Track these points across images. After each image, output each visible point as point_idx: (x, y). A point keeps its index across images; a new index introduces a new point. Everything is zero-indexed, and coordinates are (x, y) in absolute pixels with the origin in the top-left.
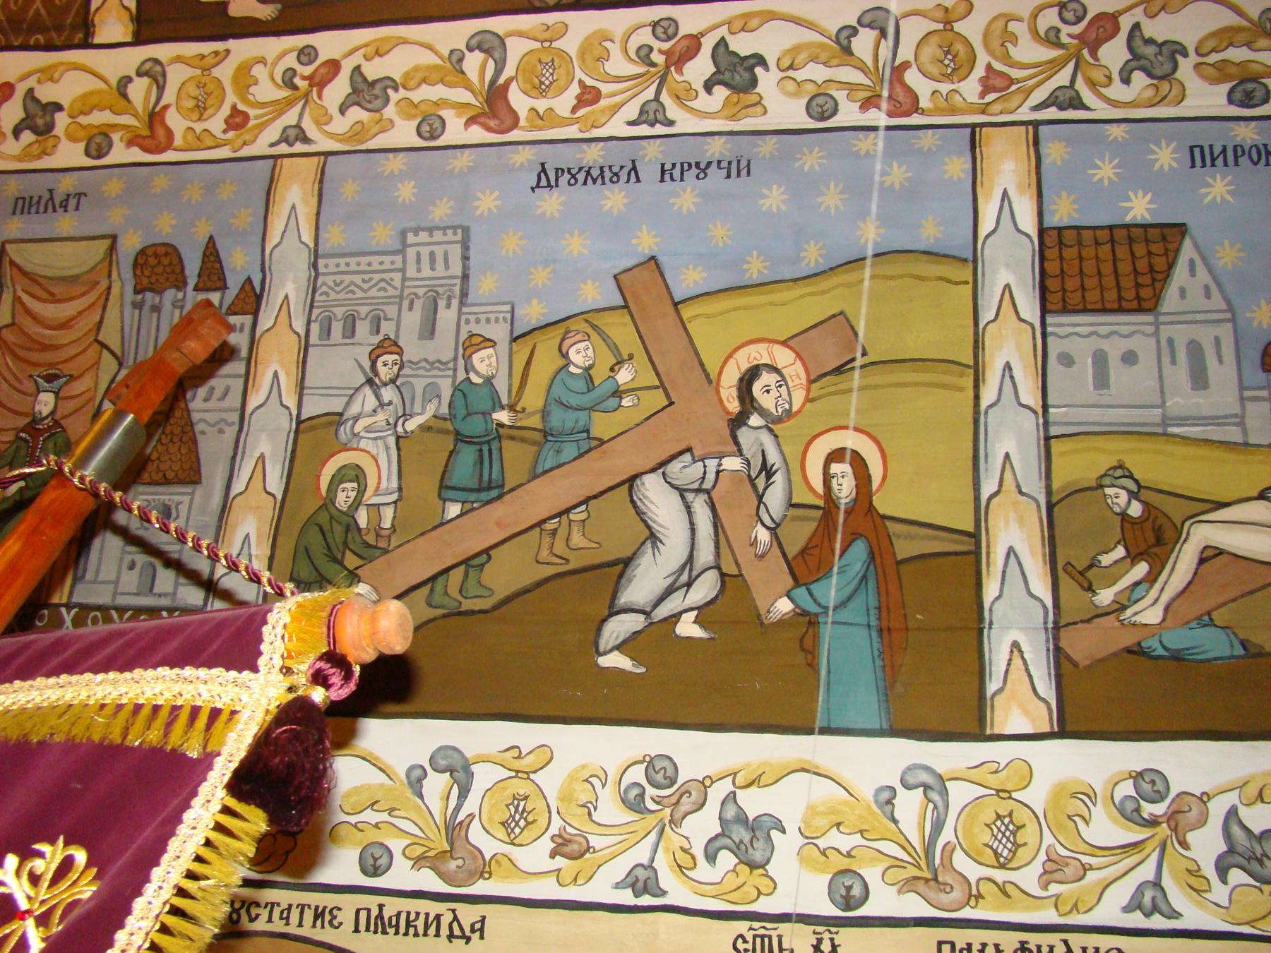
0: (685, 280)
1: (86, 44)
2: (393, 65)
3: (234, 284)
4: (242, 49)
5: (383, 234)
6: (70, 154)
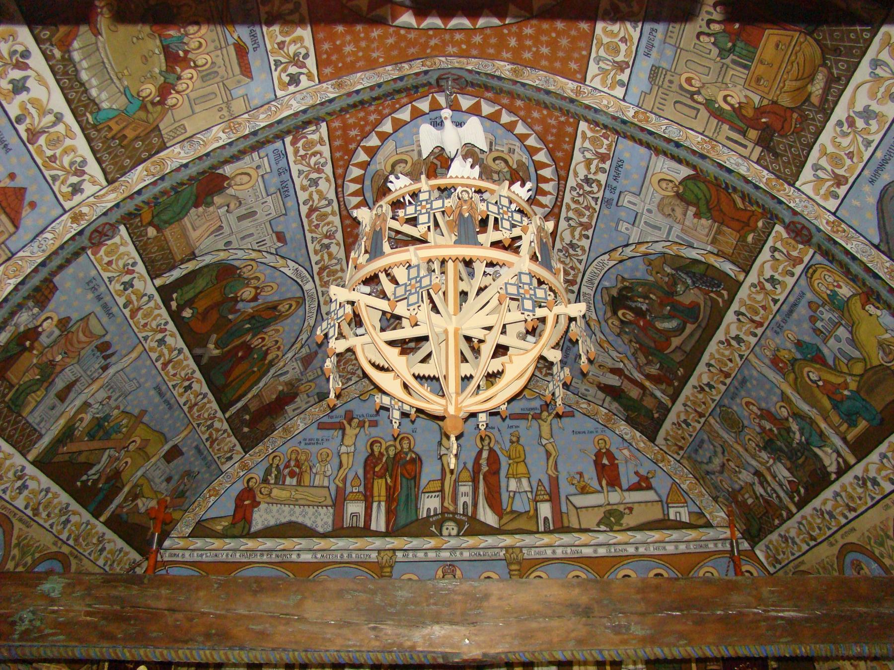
0: (146, 419)
1: (152, 279)
2: (169, 340)
3: (109, 360)
4: (163, 311)
6: (121, 301)
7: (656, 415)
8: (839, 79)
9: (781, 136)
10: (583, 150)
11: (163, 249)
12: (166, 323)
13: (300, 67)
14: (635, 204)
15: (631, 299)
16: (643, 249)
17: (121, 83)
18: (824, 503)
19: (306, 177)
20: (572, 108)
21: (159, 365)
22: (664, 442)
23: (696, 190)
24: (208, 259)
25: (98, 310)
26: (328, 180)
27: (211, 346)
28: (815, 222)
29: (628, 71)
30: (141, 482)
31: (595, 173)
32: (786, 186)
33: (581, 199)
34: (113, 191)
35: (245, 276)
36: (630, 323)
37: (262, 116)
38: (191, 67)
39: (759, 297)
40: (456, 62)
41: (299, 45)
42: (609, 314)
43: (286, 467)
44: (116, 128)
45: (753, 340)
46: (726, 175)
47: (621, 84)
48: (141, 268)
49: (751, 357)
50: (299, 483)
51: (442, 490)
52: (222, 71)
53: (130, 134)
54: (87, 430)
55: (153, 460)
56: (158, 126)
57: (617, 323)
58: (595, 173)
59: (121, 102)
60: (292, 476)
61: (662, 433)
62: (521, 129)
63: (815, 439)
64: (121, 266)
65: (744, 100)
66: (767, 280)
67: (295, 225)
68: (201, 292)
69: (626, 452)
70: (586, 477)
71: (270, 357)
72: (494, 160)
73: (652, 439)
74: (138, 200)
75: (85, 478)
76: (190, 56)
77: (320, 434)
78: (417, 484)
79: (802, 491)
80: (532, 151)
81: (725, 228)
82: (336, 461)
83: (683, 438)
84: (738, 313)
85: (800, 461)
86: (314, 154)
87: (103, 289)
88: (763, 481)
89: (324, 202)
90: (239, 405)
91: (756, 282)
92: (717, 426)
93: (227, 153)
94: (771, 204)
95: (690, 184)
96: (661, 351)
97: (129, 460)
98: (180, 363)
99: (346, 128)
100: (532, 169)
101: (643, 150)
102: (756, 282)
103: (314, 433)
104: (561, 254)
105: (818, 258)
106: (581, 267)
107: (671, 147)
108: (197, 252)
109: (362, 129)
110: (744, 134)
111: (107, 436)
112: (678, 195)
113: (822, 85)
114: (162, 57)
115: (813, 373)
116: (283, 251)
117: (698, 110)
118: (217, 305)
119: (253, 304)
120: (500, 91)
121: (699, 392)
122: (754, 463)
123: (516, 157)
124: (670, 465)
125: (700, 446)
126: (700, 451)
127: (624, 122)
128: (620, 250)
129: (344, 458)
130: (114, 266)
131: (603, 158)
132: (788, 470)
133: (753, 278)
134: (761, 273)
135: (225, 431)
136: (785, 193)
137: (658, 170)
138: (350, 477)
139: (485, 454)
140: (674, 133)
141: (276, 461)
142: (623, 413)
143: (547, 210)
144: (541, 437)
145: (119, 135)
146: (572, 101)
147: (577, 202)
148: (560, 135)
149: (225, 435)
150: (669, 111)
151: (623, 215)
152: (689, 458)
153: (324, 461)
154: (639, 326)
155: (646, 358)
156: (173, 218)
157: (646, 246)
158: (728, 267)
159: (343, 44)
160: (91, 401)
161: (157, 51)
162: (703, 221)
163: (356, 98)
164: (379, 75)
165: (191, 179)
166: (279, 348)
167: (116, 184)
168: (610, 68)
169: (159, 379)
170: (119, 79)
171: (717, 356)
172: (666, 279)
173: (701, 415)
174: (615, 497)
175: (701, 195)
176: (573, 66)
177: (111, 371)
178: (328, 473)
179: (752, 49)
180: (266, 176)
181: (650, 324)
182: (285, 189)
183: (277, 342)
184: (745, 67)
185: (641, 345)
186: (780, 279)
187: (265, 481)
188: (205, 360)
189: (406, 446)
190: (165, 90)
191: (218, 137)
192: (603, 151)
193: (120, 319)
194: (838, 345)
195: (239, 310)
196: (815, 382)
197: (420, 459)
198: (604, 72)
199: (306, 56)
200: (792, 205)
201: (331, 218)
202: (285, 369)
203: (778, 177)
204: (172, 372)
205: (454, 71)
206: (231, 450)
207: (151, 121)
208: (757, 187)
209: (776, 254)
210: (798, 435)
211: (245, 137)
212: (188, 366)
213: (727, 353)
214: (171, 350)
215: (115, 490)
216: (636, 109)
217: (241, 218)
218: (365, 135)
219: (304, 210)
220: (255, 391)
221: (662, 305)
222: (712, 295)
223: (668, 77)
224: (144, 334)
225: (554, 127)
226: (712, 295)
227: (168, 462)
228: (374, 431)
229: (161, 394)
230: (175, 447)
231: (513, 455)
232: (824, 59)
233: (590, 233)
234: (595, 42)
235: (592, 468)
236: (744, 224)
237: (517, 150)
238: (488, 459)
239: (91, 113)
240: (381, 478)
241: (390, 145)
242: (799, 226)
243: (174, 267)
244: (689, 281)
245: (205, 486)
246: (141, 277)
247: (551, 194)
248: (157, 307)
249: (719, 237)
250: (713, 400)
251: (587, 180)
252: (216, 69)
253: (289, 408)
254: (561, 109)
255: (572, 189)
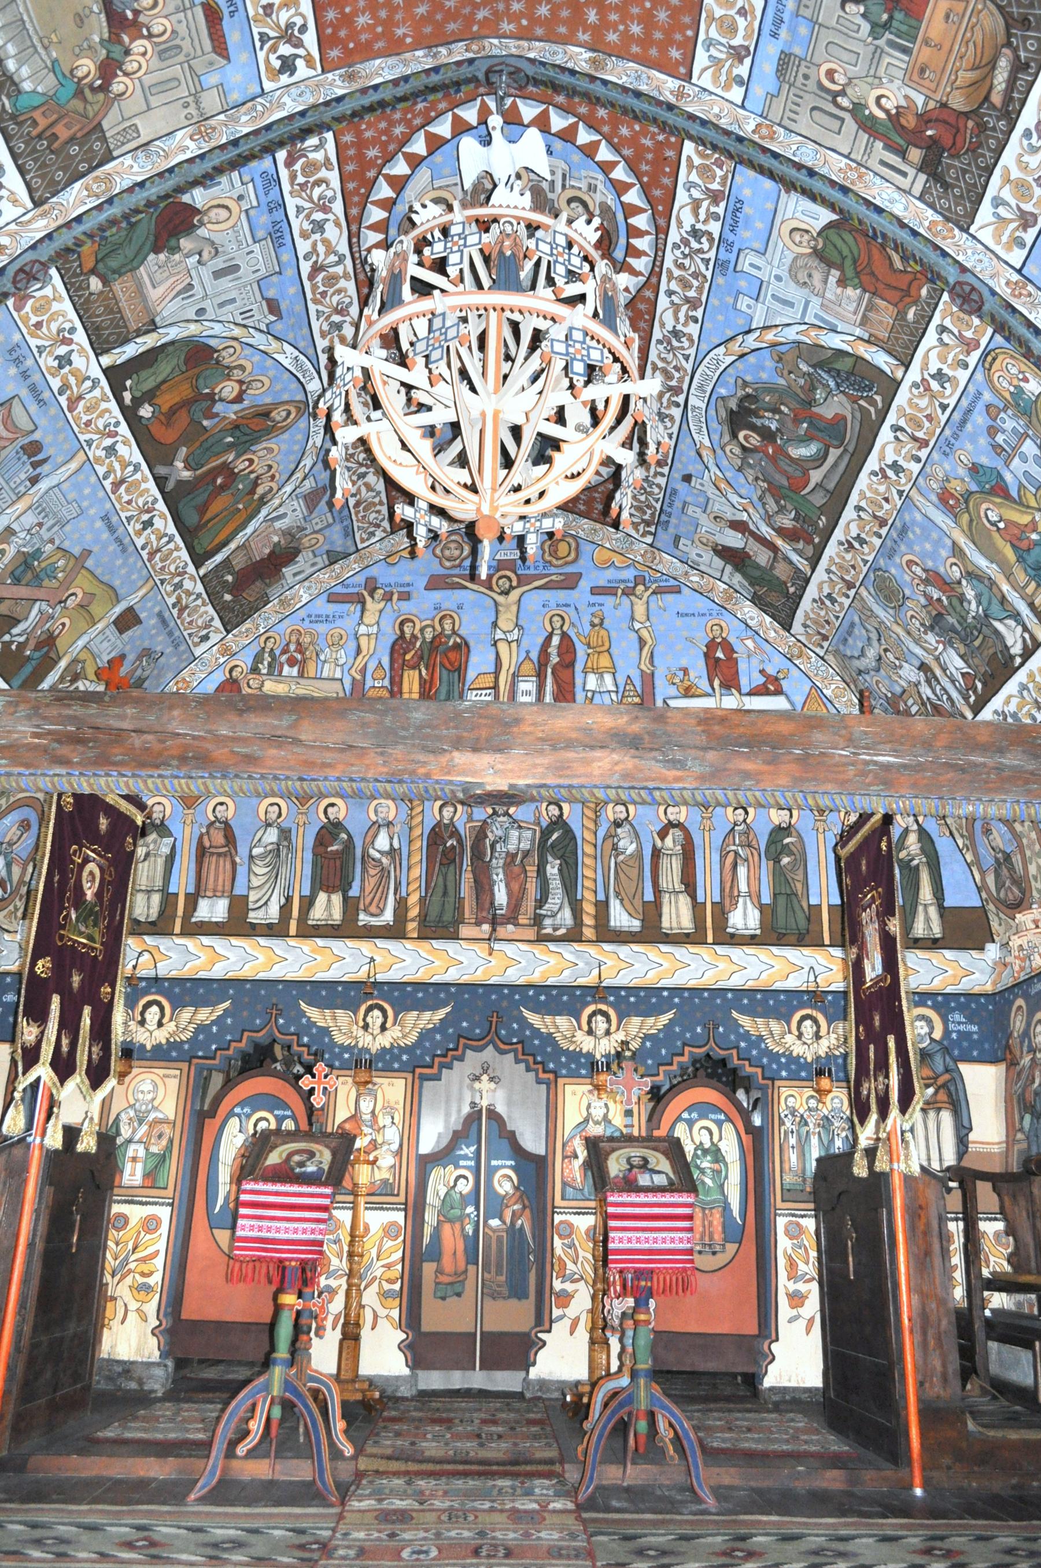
0: (89, 563)
1: (97, 355)
4: (113, 405)
5: (71, 496)
6: (56, 383)
7: (792, 590)
8: (1027, 66)
9: (951, 156)
10: (690, 186)
11: (112, 312)
12: (117, 424)
13: (295, 46)
14: (759, 268)
15: (755, 413)
16: (770, 336)
17: (49, 55)
18: (1007, 702)
19: (308, 217)
20: (671, 118)
21: (107, 484)
22: (802, 630)
23: (839, 243)
24: (173, 333)
25: (24, 393)
26: (337, 224)
27: (179, 464)
28: (991, 283)
29: (748, 61)
30: (82, 657)
31: (705, 222)
32: (956, 231)
33: (687, 262)
34: (44, 215)
35: (226, 362)
36: (754, 450)
37: (244, 119)
38: (143, 37)
39: (923, 403)
40: (512, 46)
41: (292, 11)
42: (727, 438)
43: (284, 652)
44: (43, 123)
45: (915, 468)
46: (875, 216)
47: (740, 81)
48: (81, 337)
49: (914, 493)
50: (301, 675)
51: (495, 687)
52: (186, 45)
53: (63, 133)
54: (10, 569)
55: (100, 626)
56: (100, 124)
57: (737, 451)
58: (705, 222)
59: (47, 84)
60: (291, 665)
61: (800, 615)
62: (605, 154)
63: (995, 608)
64: (54, 331)
65: (903, 103)
66: (933, 377)
67: (293, 290)
68: (164, 382)
69: (749, 643)
70: (692, 674)
71: (260, 490)
72: (569, 201)
73: (787, 626)
74: (78, 230)
75: (7, 638)
76: (142, 19)
77: (332, 608)
78: (462, 679)
79: (979, 685)
80: (620, 188)
81: (878, 301)
82: (352, 645)
83: (828, 622)
84: (896, 428)
85: (977, 643)
86: (318, 183)
87: (29, 362)
88: (931, 679)
89: (333, 258)
90: (219, 558)
91: (918, 380)
92: (871, 601)
93: (198, 170)
94: (933, 257)
95: (832, 234)
96: (797, 491)
97: (67, 621)
98: (137, 484)
99: (361, 144)
100: (620, 217)
101: (768, 184)
102: (918, 380)
103: (322, 607)
104: (661, 347)
105: (999, 339)
106: (688, 367)
107: (802, 177)
108: (157, 319)
109: (384, 146)
110: (903, 154)
111: (37, 580)
112: (816, 253)
113: (1006, 75)
114: (103, 16)
115: (992, 512)
116: (278, 328)
117: (843, 120)
118: (186, 404)
119: (236, 407)
120: (572, 92)
121: (847, 551)
122: (918, 651)
123: (598, 197)
124: (811, 663)
125: (850, 633)
126: (850, 641)
127: (740, 139)
128: (740, 338)
129: (363, 641)
130: (44, 329)
131: (715, 197)
132: (961, 657)
133: (914, 374)
134: (925, 366)
135: (199, 596)
136: (958, 245)
137: (789, 214)
138: (372, 666)
139: (556, 640)
140: (807, 155)
141: (270, 645)
142: (748, 590)
143: (642, 279)
144: (633, 619)
145: (48, 133)
146: (670, 107)
147: (681, 267)
148: (660, 161)
149: (199, 602)
150: (804, 123)
151: (743, 284)
152: (837, 653)
153: (336, 644)
154: (767, 454)
155: (777, 502)
156: (123, 266)
157: (774, 331)
158: (881, 360)
159: (355, 13)
160: (15, 526)
161: (95, 9)
162: (849, 291)
163: (373, 97)
164: (406, 64)
165: (149, 204)
166: (273, 477)
167: (46, 207)
168: (723, 56)
169: (108, 505)
170: (46, 48)
171: (868, 494)
172: (802, 382)
173: (850, 585)
174: (730, 702)
175: (846, 252)
176: (675, 54)
177: (43, 485)
178: (342, 661)
179: (914, 23)
180: (252, 212)
181: (781, 451)
182: (278, 235)
183: (270, 467)
184: (905, 51)
185: (769, 483)
186: (950, 373)
187: (255, 670)
188: (170, 486)
189: (448, 627)
190: (109, 69)
191: (185, 146)
192: (715, 186)
193: (53, 410)
194: (1025, 467)
195: (217, 415)
196: (994, 524)
197: (467, 644)
198: (717, 63)
199: (303, 29)
200: (960, 258)
201: (342, 283)
202: (282, 511)
203: (948, 219)
204: (126, 498)
205: (512, 61)
206: (207, 626)
207: (91, 114)
208: (915, 233)
209: (945, 337)
210: (974, 606)
211: (222, 147)
212: (147, 490)
213: (882, 489)
214: (125, 465)
215: (48, 663)
216: (759, 120)
217: (218, 274)
218: (389, 158)
219: (306, 267)
220: (239, 539)
221: (797, 421)
222: (862, 402)
223: (803, 70)
224: (87, 437)
225: (648, 150)
226: (862, 402)
227: (121, 632)
228: (405, 607)
229: (112, 529)
230: (130, 609)
231: (594, 642)
232: (1009, 35)
233: (699, 313)
234: (704, 15)
235: (701, 663)
236: (905, 295)
237: (600, 187)
238: (559, 647)
239: (9, 97)
240: (413, 668)
241: (424, 174)
242: (967, 289)
243: (126, 341)
244: (832, 384)
245: (170, 675)
246: (82, 350)
247: (645, 254)
248: (104, 399)
249: (871, 315)
250: (865, 562)
251: (695, 233)
252: (178, 42)
253: (288, 571)
254: (655, 120)
255: (676, 246)
